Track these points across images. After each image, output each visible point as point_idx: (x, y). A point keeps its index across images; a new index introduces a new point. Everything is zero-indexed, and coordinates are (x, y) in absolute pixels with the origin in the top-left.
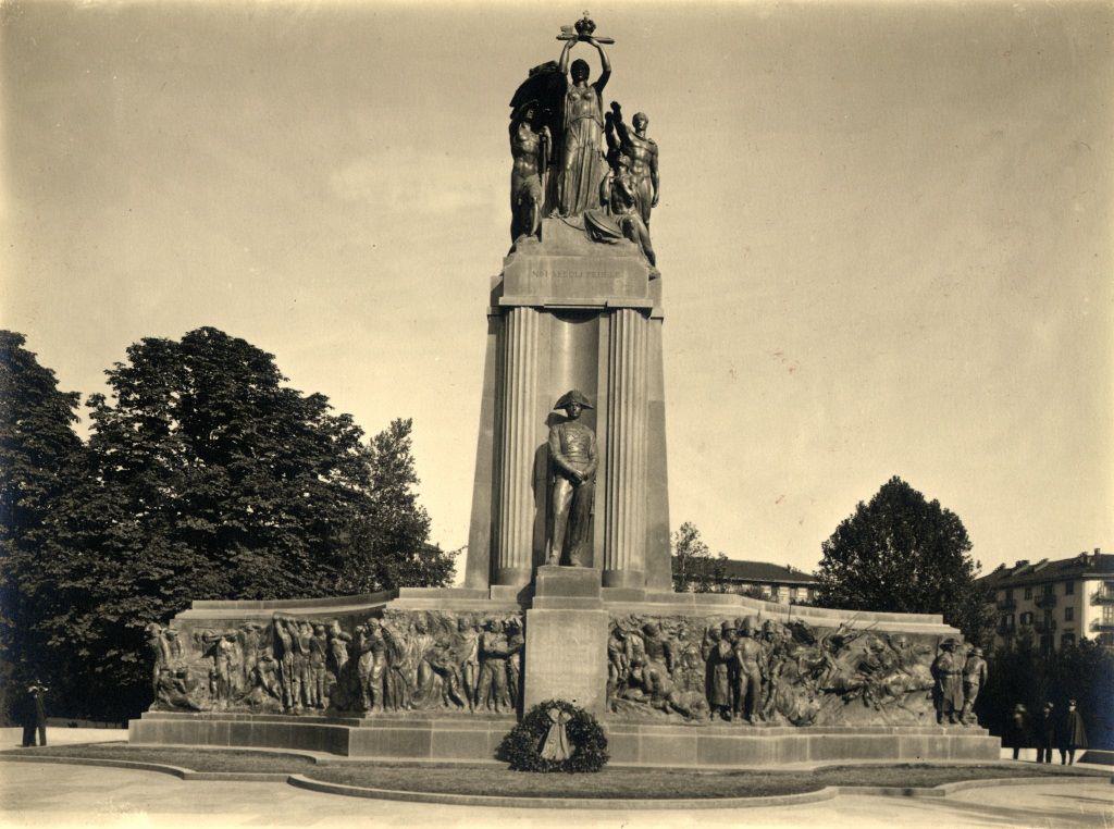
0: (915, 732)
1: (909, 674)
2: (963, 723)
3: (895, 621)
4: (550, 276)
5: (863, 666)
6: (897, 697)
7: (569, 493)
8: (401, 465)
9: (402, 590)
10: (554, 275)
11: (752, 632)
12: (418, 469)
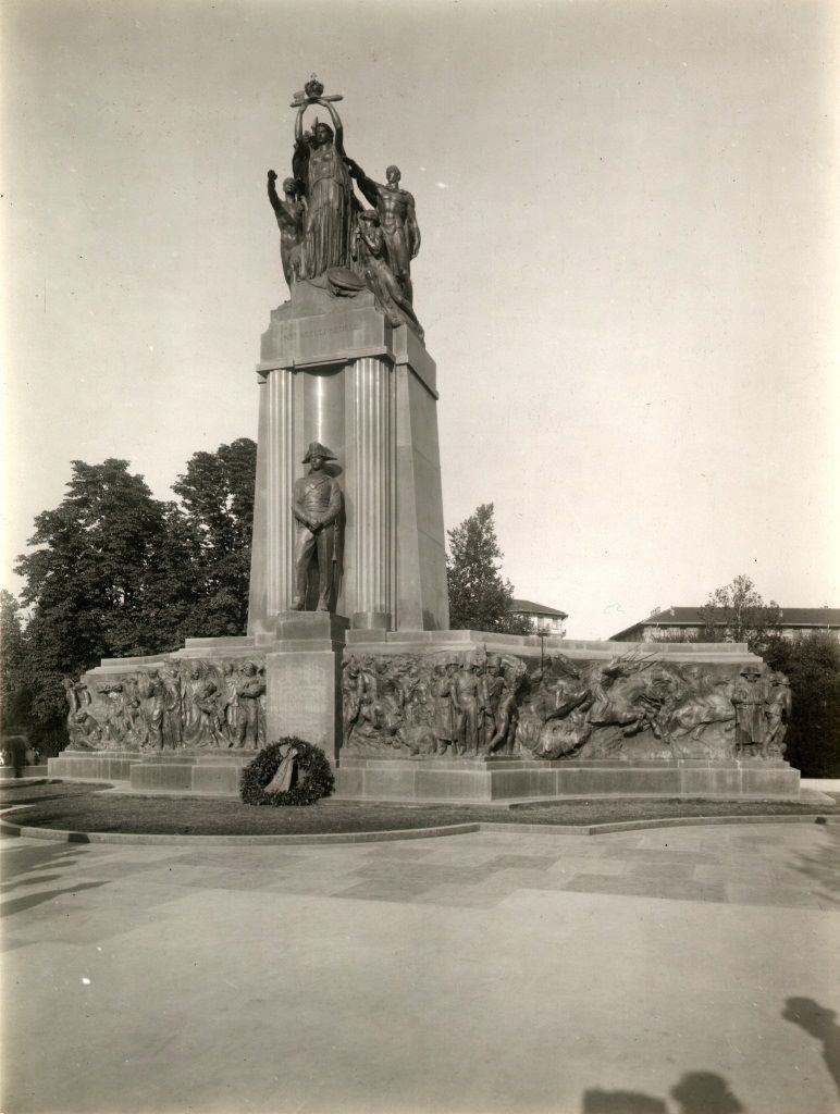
0: (705, 765)
1: (702, 705)
2: (763, 756)
3: (692, 651)
4: (298, 336)
5: (638, 699)
6: (690, 730)
7: (310, 541)
8: (487, 543)
9: (188, 641)
10: (302, 335)
11: (468, 667)
12: (500, 544)
